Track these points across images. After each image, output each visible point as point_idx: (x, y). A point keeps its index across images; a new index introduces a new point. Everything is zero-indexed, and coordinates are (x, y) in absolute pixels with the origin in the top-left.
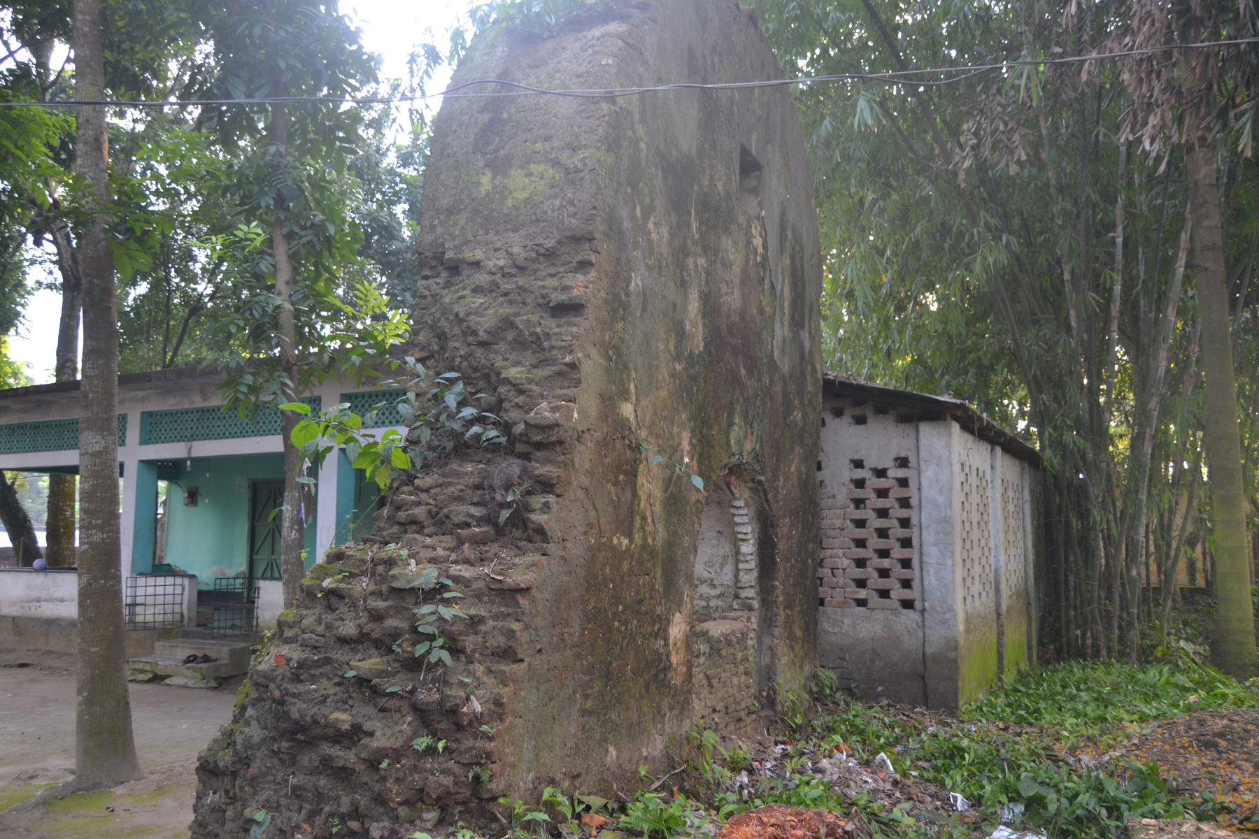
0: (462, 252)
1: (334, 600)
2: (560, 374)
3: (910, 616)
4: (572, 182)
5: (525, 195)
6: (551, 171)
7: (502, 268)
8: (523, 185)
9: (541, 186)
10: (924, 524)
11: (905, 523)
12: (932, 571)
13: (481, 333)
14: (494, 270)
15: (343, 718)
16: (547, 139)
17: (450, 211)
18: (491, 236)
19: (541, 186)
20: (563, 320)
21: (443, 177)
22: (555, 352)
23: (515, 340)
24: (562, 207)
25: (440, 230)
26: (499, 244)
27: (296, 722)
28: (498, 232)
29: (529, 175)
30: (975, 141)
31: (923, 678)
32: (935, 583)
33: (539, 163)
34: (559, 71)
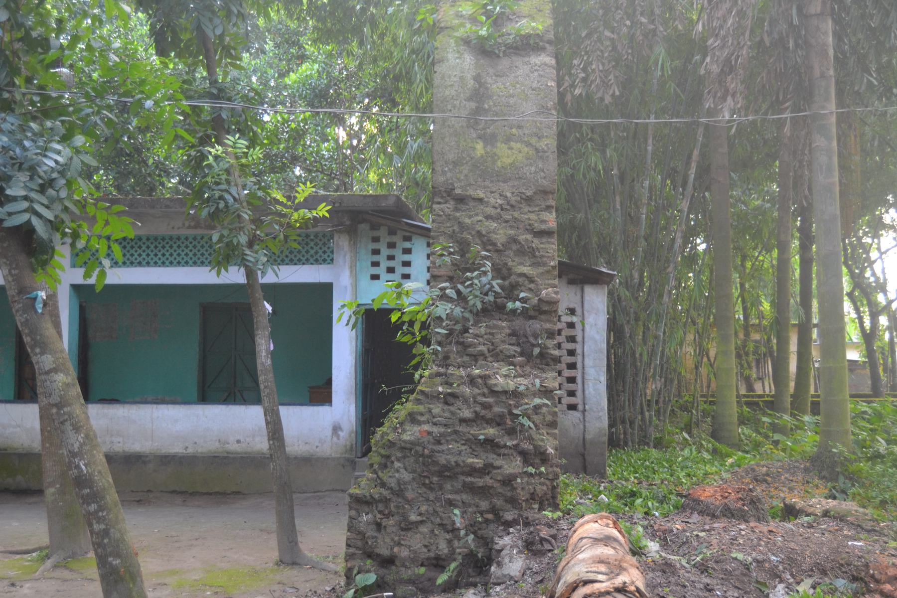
0: (467, 191)
1: (451, 400)
2: (548, 272)
3: (575, 415)
4: (541, 157)
5: (510, 161)
6: (526, 149)
7: (501, 205)
8: (508, 155)
9: (520, 157)
10: (586, 353)
11: (572, 353)
12: (591, 384)
13: (499, 245)
14: (497, 205)
15: (478, 462)
16: (519, 127)
17: (456, 164)
18: (487, 183)
19: (520, 157)
20: (544, 240)
21: (447, 140)
22: (545, 259)
23: (518, 250)
24: (535, 172)
25: (449, 175)
26: (494, 189)
27: (444, 466)
28: (492, 182)
29: (511, 148)
30: (583, 75)
31: (583, 455)
32: (593, 392)
33: (517, 142)
34: (518, 83)
